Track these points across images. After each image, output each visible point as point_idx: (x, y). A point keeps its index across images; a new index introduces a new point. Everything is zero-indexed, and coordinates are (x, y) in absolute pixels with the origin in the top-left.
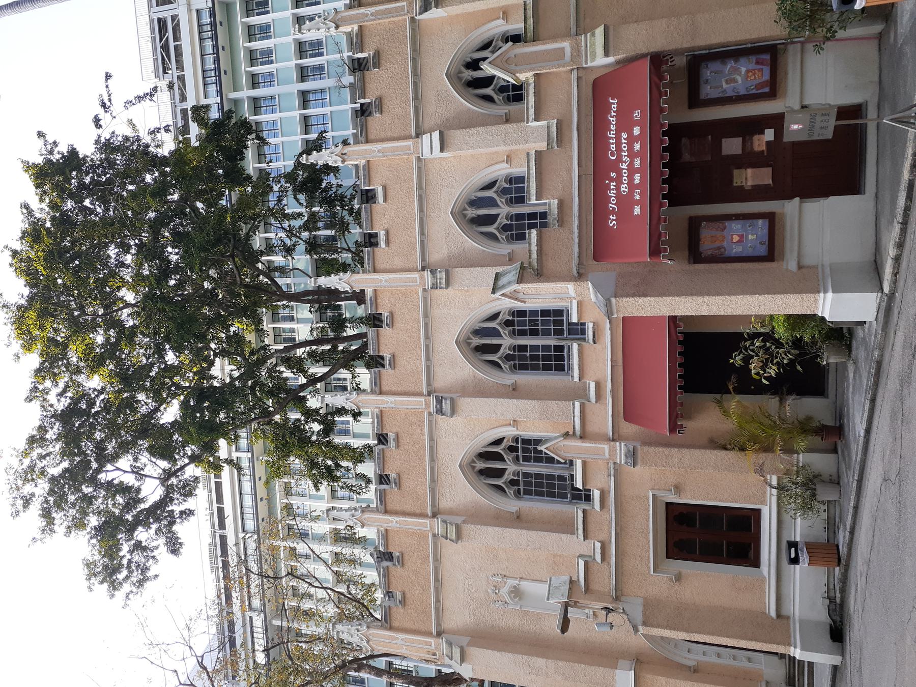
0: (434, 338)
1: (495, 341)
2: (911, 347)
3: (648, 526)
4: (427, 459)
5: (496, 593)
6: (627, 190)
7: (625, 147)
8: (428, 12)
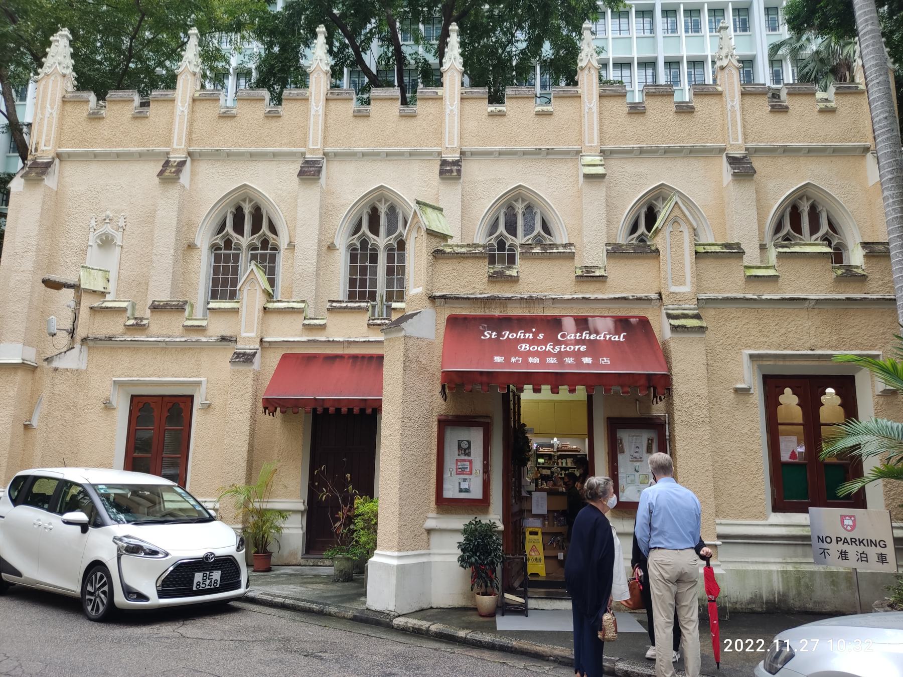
0: (388, 162)
1: (383, 229)
2: (320, 652)
3: (166, 376)
4: (253, 149)
5: (105, 220)
6: (522, 349)
7: (570, 348)
8: (729, 166)
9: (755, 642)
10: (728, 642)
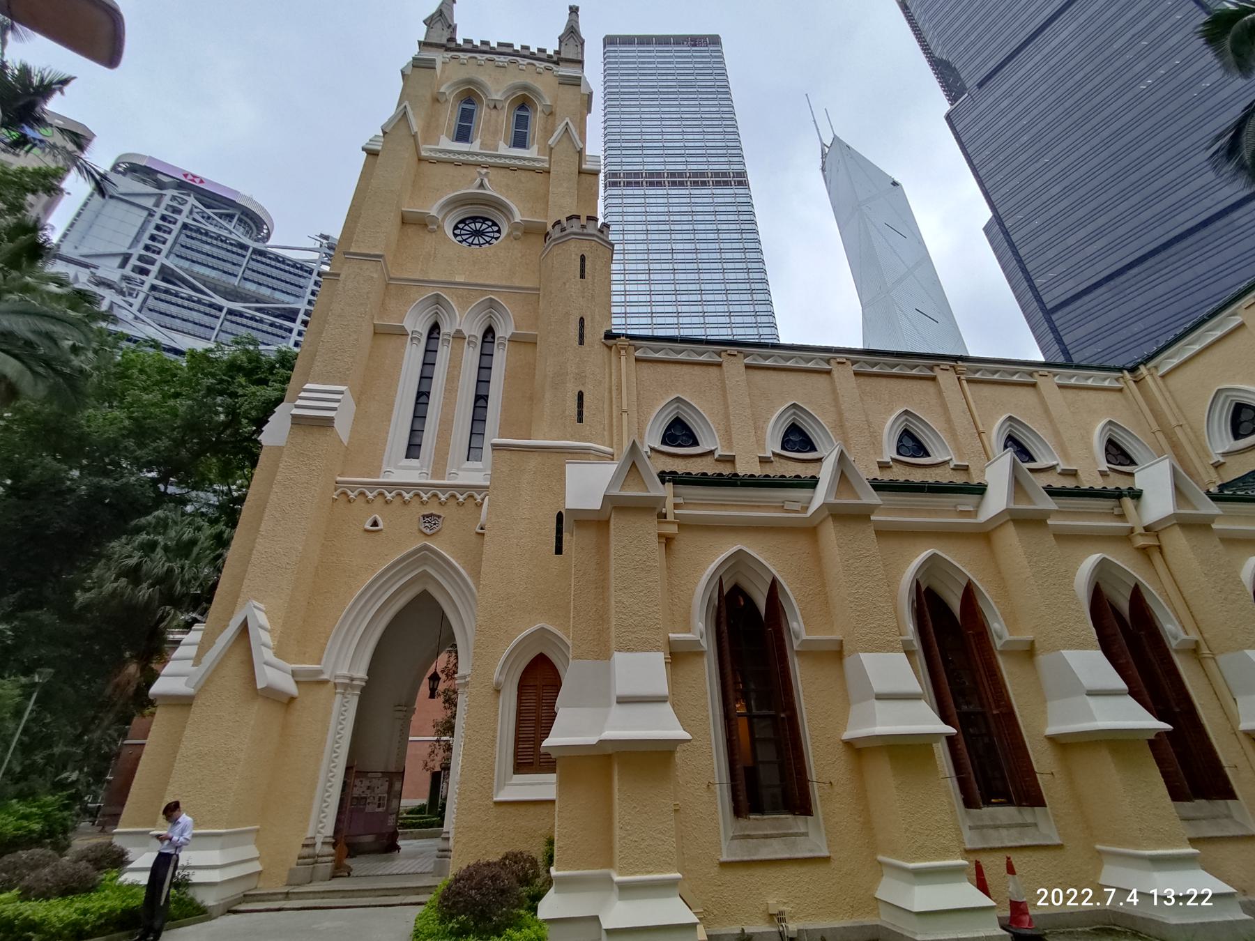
9: (1079, 892)
10: (1043, 893)
